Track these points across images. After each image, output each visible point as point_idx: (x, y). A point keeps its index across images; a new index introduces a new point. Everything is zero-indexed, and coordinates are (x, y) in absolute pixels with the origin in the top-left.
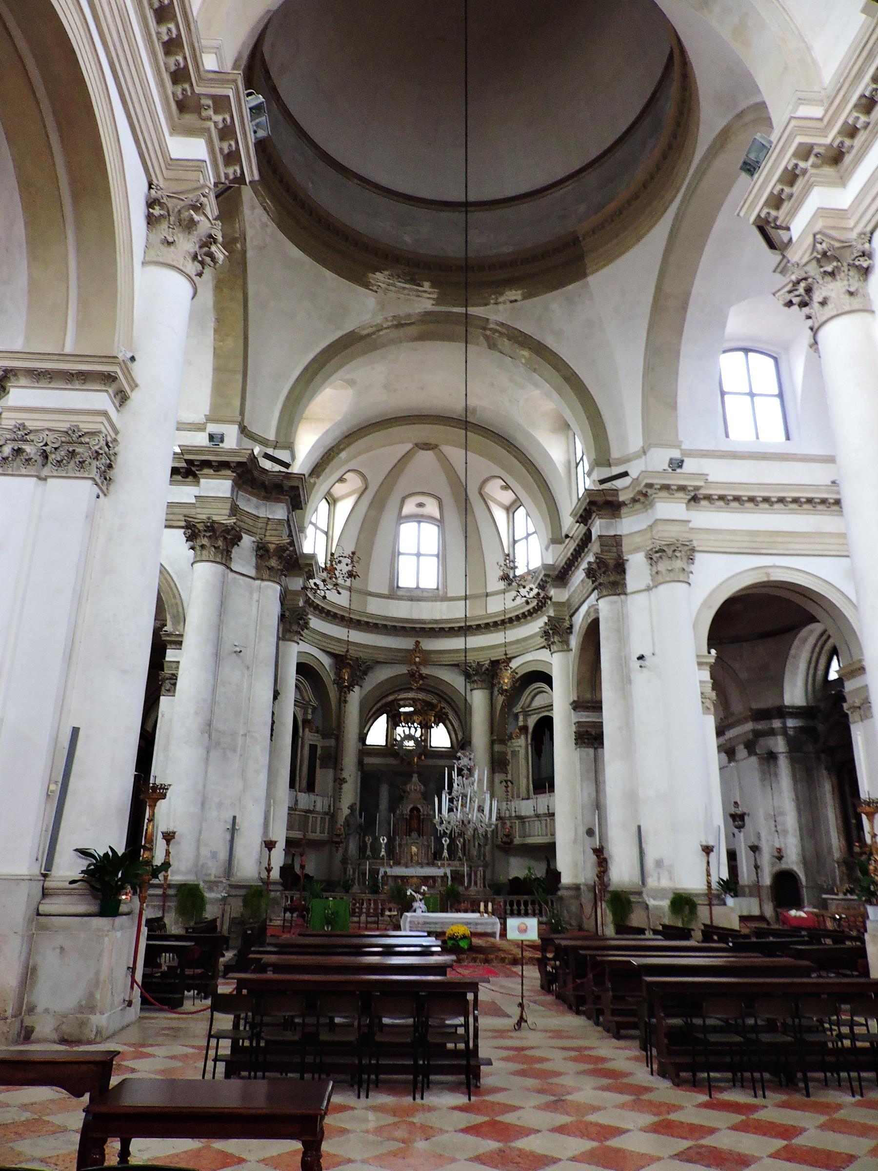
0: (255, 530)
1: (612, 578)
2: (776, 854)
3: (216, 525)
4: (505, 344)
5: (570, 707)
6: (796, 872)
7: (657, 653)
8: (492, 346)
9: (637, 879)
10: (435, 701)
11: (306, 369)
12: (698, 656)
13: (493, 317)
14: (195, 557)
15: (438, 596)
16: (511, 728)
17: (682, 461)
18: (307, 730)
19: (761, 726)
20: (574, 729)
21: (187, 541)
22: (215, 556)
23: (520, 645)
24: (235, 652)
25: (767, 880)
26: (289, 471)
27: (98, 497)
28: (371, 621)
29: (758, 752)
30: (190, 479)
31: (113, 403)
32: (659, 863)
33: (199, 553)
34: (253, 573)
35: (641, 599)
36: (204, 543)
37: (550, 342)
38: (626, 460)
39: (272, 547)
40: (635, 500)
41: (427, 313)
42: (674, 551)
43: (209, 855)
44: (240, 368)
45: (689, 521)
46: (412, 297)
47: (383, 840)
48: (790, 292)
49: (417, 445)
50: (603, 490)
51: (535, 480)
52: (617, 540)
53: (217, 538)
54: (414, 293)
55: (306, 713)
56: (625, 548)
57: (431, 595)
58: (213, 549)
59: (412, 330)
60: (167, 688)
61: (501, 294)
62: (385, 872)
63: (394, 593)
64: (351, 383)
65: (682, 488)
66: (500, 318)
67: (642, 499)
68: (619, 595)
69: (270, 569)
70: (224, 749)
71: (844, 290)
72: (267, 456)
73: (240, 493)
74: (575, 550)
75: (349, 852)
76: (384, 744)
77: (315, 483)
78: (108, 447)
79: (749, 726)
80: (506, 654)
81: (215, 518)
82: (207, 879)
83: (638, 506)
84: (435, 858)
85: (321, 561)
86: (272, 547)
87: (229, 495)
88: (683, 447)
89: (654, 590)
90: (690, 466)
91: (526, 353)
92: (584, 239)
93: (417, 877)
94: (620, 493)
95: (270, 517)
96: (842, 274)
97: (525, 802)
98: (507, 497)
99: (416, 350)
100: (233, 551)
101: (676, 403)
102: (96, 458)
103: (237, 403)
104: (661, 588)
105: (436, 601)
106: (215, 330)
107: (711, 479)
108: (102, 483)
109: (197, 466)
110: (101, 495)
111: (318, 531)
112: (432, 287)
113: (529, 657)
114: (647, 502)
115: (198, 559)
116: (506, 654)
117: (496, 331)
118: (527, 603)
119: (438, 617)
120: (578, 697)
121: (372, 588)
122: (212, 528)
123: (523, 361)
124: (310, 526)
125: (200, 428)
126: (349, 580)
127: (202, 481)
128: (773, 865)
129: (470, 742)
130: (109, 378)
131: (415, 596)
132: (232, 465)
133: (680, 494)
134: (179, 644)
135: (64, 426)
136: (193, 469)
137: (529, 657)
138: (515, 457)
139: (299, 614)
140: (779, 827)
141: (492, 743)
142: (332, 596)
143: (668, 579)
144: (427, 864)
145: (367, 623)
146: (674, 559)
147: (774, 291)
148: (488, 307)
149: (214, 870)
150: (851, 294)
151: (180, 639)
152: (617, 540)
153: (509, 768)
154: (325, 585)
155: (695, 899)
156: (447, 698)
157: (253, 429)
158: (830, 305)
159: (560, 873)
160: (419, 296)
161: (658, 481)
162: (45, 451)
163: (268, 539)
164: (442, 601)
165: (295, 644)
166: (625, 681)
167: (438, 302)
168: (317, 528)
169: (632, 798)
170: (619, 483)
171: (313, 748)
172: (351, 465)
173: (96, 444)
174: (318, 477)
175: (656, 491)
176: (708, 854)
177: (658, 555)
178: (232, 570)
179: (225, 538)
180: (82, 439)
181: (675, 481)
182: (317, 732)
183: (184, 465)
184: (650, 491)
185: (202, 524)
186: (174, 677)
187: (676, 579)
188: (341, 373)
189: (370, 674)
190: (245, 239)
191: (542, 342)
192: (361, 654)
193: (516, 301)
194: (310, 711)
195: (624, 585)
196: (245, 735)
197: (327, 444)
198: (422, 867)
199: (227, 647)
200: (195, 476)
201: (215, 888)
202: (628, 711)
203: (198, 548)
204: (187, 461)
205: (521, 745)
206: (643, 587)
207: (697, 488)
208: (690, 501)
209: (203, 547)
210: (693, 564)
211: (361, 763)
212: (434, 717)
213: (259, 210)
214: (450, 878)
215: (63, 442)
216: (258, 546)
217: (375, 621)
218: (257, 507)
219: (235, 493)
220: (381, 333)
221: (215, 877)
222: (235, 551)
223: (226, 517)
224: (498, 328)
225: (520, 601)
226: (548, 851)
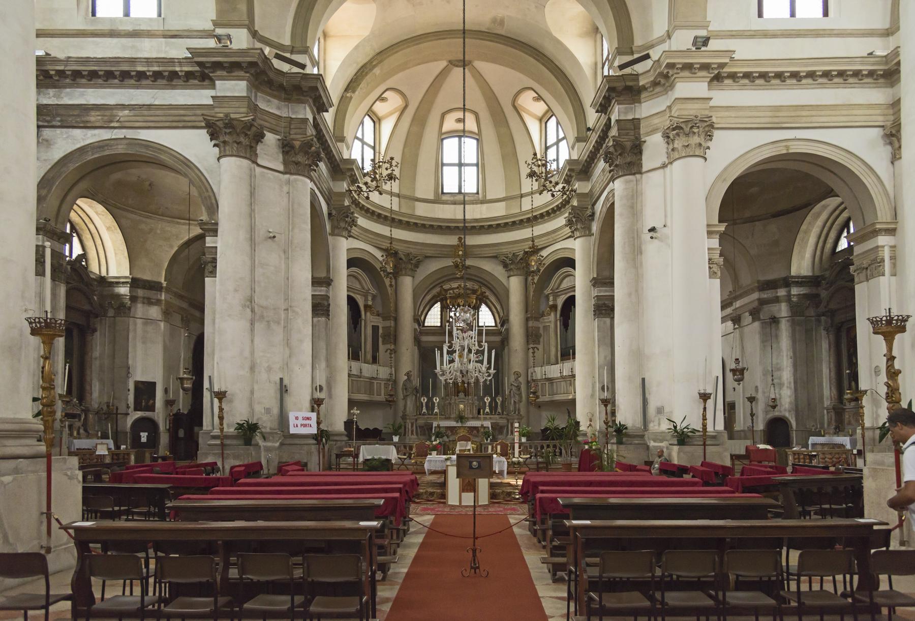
0: (278, 129)
1: (629, 160)
2: (771, 404)
3: (235, 123)
6: (787, 418)
10: (476, 287)
14: (220, 152)
15: (480, 199)
18: (368, 314)
19: (765, 295)
23: (550, 237)
25: (760, 426)
29: (762, 317)
34: (281, 168)
35: (656, 176)
39: (297, 144)
55: (366, 300)
57: (472, 198)
58: (236, 145)
63: (440, 197)
68: (634, 174)
76: (439, 324)
79: (755, 296)
86: (297, 144)
100: (259, 148)
104: (676, 164)
105: (477, 203)
115: (222, 154)
121: (419, 194)
126: (389, 183)
128: (767, 412)
139: (344, 213)
140: (775, 381)
141: (527, 320)
142: (375, 197)
145: (416, 224)
153: (541, 340)
154: (367, 188)
156: (486, 283)
165: (345, 239)
171: (375, 329)
178: (258, 165)
182: (378, 316)
185: (221, 122)
187: (691, 154)
192: (412, 250)
194: (370, 298)
195: (640, 165)
203: (222, 145)
205: (552, 320)
206: (659, 165)
211: (417, 341)
216: (283, 144)
217: (422, 222)
222: (259, 148)
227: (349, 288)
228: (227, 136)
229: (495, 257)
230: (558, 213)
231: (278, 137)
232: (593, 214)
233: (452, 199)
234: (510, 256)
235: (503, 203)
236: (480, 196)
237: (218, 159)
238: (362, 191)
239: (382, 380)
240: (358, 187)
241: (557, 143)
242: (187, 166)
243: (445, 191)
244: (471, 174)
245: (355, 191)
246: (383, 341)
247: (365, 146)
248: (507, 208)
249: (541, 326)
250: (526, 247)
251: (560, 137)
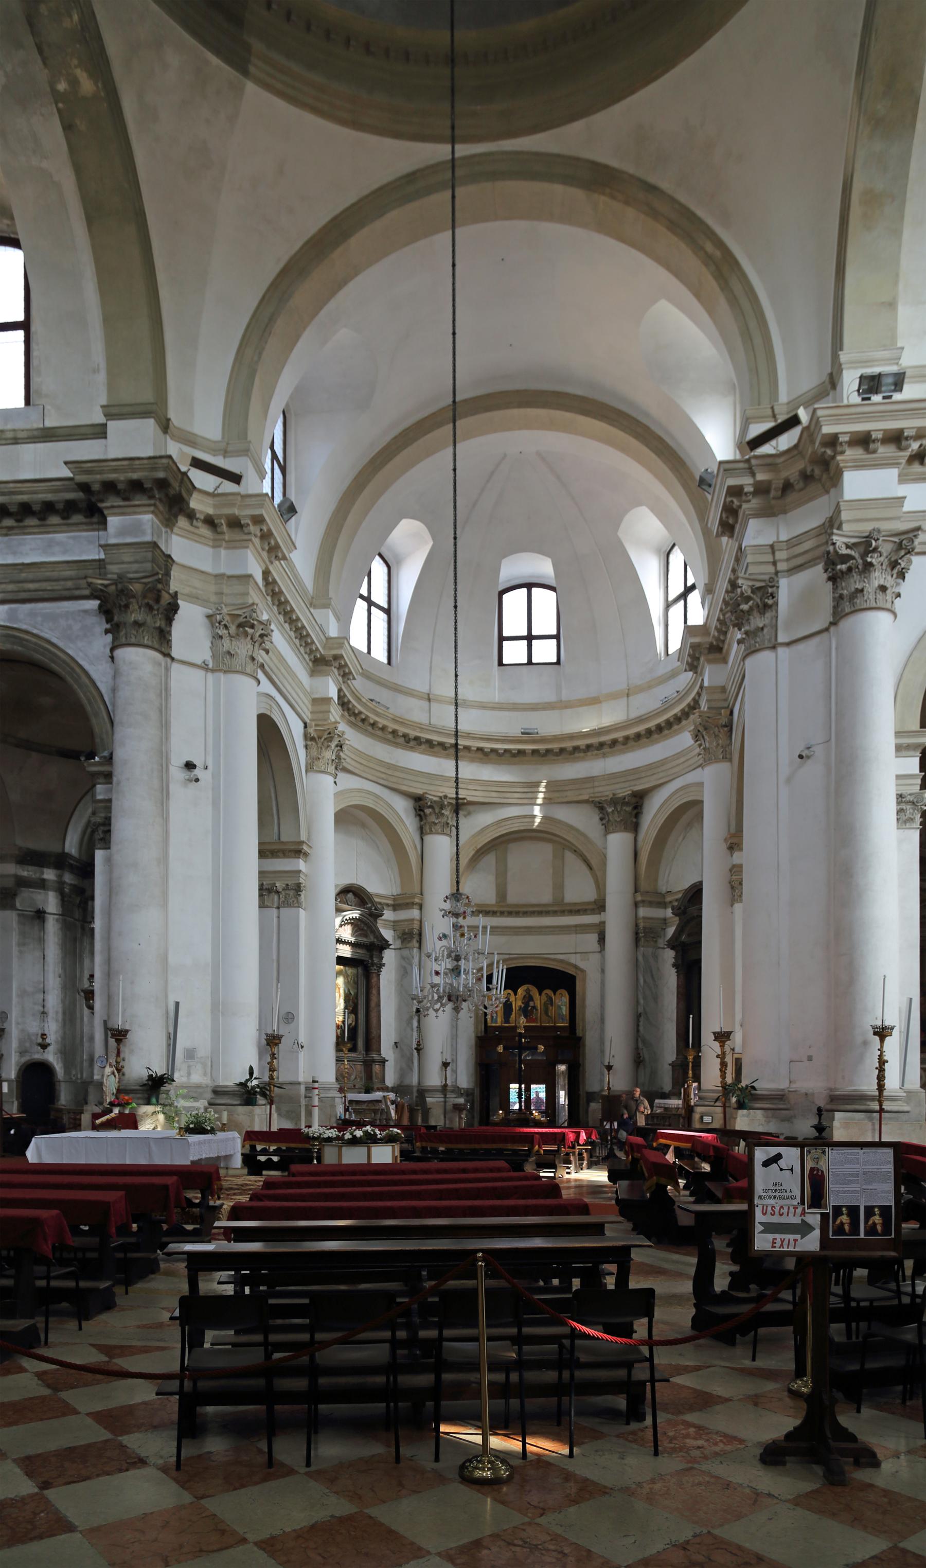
72: (198, 464)
111: (373, 608)
168: (370, 603)
241: (684, 596)
247: (373, 609)
251: (689, 584)
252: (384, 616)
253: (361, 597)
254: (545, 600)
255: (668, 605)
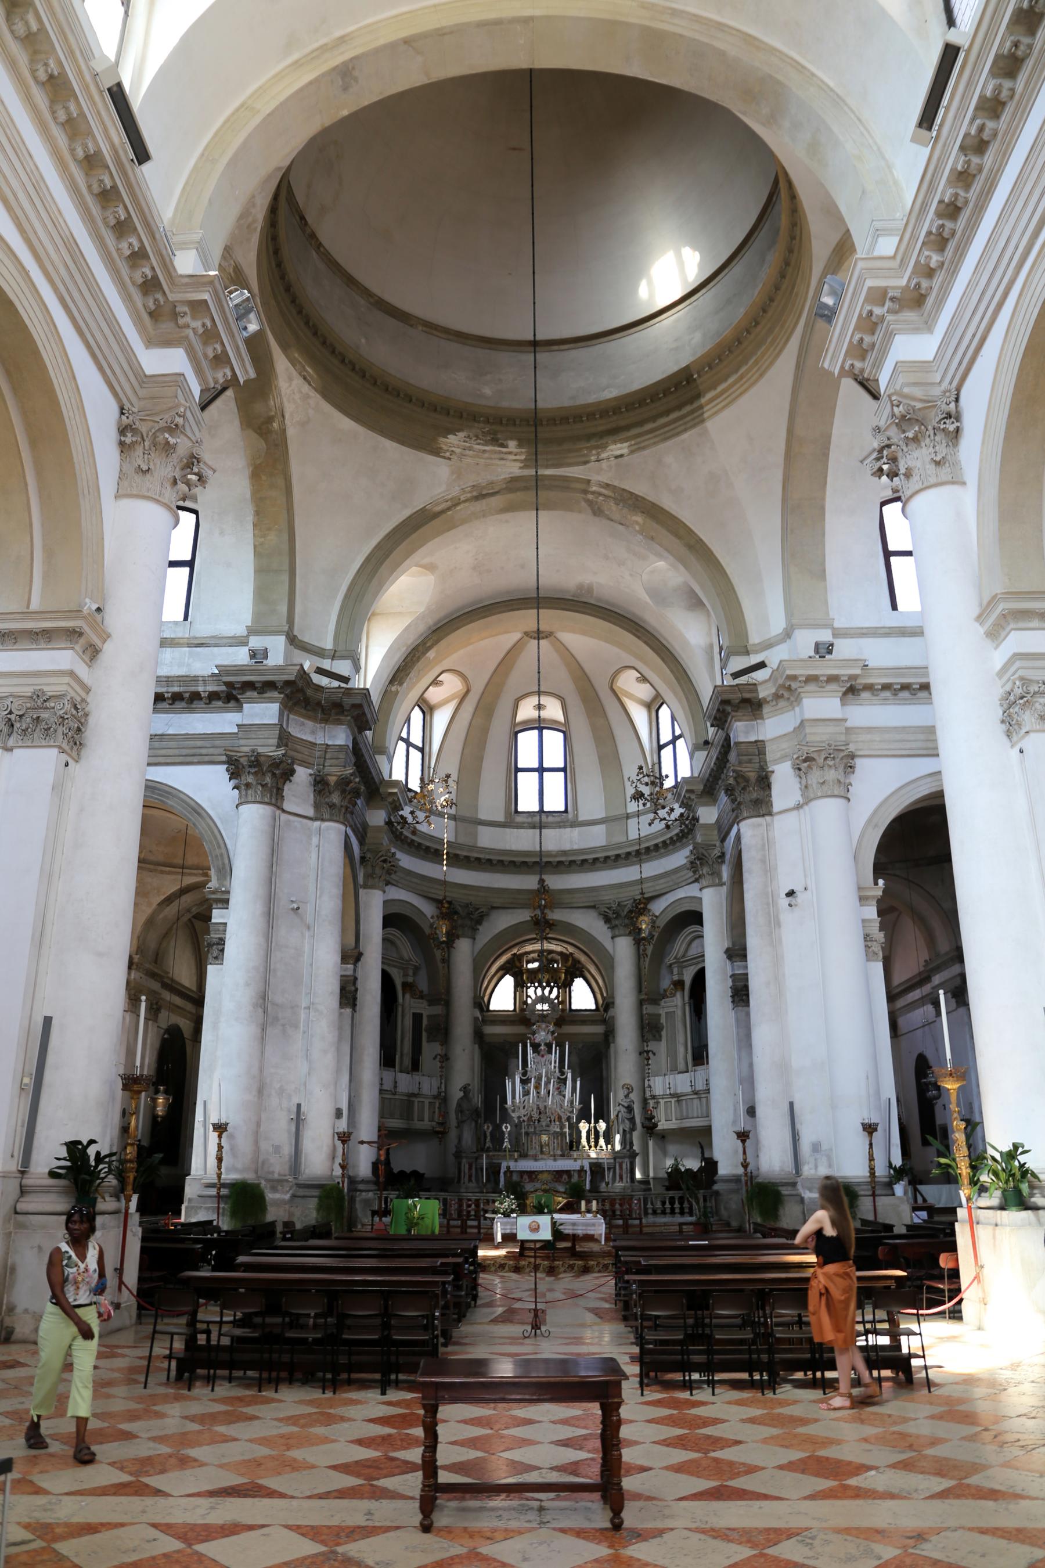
0: (311, 760)
1: (754, 796)
3: (262, 759)
4: (612, 508)
5: (725, 956)
7: (809, 888)
8: (597, 512)
9: (790, 1167)
11: (368, 559)
12: (860, 889)
13: (595, 478)
14: (240, 798)
16: (666, 983)
17: (832, 645)
18: (408, 996)
20: (730, 983)
21: (230, 779)
22: (263, 796)
23: (668, 879)
24: (293, 909)
26: (349, 686)
27: (67, 765)
28: (481, 856)
30: (232, 704)
31: (82, 659)
32: (816, 1147)
33: (244, 793)
34: (310, 812)
35: (792, 818)
36: (250, 781)
37: (668, 503)
38: (768, 645)
39: (332, 780)
40: (777, 696)
41: (514, 480)
42: (826, 758)
43: (271, 1149)
44: (286, 567)
45: (846, 720)
46: (494, 462)
47: (506, 1128)
48: (878, 459)
49: (526, 634)
50: (737, 685)
51: (672, 671)
52: (759, 747)
53: (263, 774)
54: (497, 456)
55: (406, 975)
56: (769, 757)
58: (260, 787)
59: (494, 501)
60: (215, 955)
61: (604, 447)
62: (508, 1168)
63: (513, 818)
64: (431, 568)
65: (833, 679)
66: (604, 478)
67: (786, 695)
68: (763, 816)
69: (332, 806)
70: (283, 1025)
71: (928, 459)
72: (320, 671)
73: (291, 716)
74: (717, 758)
75: (464, 1143)
76: (511, 1008)
77: (397, 692)
78: (76, 709)
80: (642, 893)
81: (261, 750)
82: (270, 1177)
83: (782, 703)
84: (571, 1148)
85: (414, 784)
86: (332, 780)
87: (276, 722)
88: (836, 625)
89: (806, 808)
90: (844, 649)
91: (639, 518)
92: (699, 376)
93: (549, 1172)
94: (760, 688)
95: (330, 743)
96: (928, 440)
97: (681, 1075)
98: (645, 692)
99: (507, 521)
100: (285, 788)
101: (824, 571)
102: (62, 724)
103: (283, 609)
105: (565, 827)
106: (255, 525)
107: (871, 664)
108: (72, 748)
109: (238, 688)
110: (71, 761)
111: (411, 748)
112: (520, 446)
113: (681, 893)
114: (792, 699)
115: (243, 800)
116: (642, 893)
117: (600, 494)
118: (668, 827)
119: (567, 847)
120: (734, 944)
121: (483, 816)
122: (256, 762)
123: (637, 528)
124: (400, 743)
125: (242, 642)
127: (245, 705)
129: (613, 1003)
130: (73, 634)
131: (541, 819)
132: (279, 685)
133: (833, 687)
134: (225, 902)
135: (28, 691)
136: (234, 692)
137: (681, 893)
138: (646, 643)
141: (641, 1003)
143: (819, 794)
144: (563, 1155)
145: (478, 859)
146: (826, 768)
147: (861, 458)
148: (588, 466)
149: (279, 1166)
150: (938, 463)
151: (225, 896)
152: (759, 747)
153: (664, 1033)
155: (857, 1189)
157: (306, 638)
158: (915, 478)
159: (717, 1162)
160: (502, 459)
161: (802, 672)
162: (10, 719)
163: (327, 770)
164: (571, 826)
165: (381, 893)
166: (774, 923)
167: (534, 460)
168: (409, 744)
169: (784, 1069)
170: (759, 675)
171: (417, 1018)
172: (446, 664)
173: (63, 707)
174: (401, 684)
175: (799, 684)
176: (870, 1134)
177: (806, 765)
178: (284, 811)
179: (274, 774)
180: (48, 704)
181: (824, 669)
182: (422, 997)
183: (224, 688)
184: (794, 685)
186: (222, 942)
187: (829, 793)
188: (417, 556)
189: (485, 924)
190: (283, 416)
191: (658, 503)
193: (622, 456)
194: (411, 972)
195: (769, 804)
196: (309, 1008)
197: (409, 642)
198: (555, 1160)
199: (283, 904)
200: (237, 700)
201: (280, 1188)
202: (777, 961)
204: (226, 684)
205: (677, 1004)
206: (792, 805)
207: (854, 677)
208: (845, 694)
209: (248, 786)
210: (853, 773)
211: (479, 1036)
212: (566, 974)
213: (298, 381)
214: (588, 1173)
215: (28, 709)
216: (315, 780)
217: (488, 857)
218: (313, 732)
219: (285, 718)
220: (458, 508)
221: (280, 1175)
222: (288, 789)
223: (274, 748)
224: (603, 491)
225: (659, 826)
226: (702, 1137)
227: (385, 960)
228: (251, 776)
229: (594, 907)
230: (678, 844)
231: (310, 771)
232: (723, 855)
233: (530, 820)
234: (614, 906)
235: (603, 827)
236: (570, 815)
237: (237, 807)
238: (406, 822)
239: (426, 1097)
240: (402, 817)
242: (199, 814)
243: (520, 809)
244: (555, 783)
245: (399, 823)
246: (428, 1037)
248: (609, 834)
249: (662, 1012)
250: (635, 893)
252: (419, 754)
253: (402, 739)
254: (554, 740)
255: (660, 747)
